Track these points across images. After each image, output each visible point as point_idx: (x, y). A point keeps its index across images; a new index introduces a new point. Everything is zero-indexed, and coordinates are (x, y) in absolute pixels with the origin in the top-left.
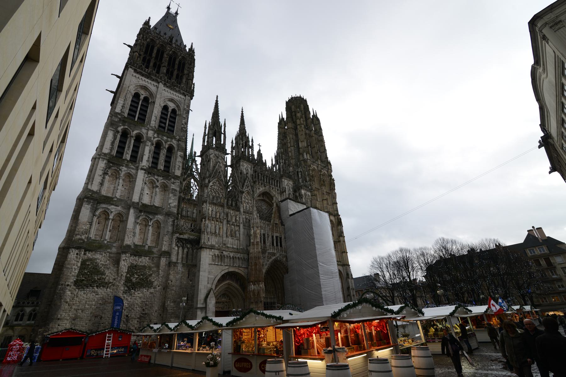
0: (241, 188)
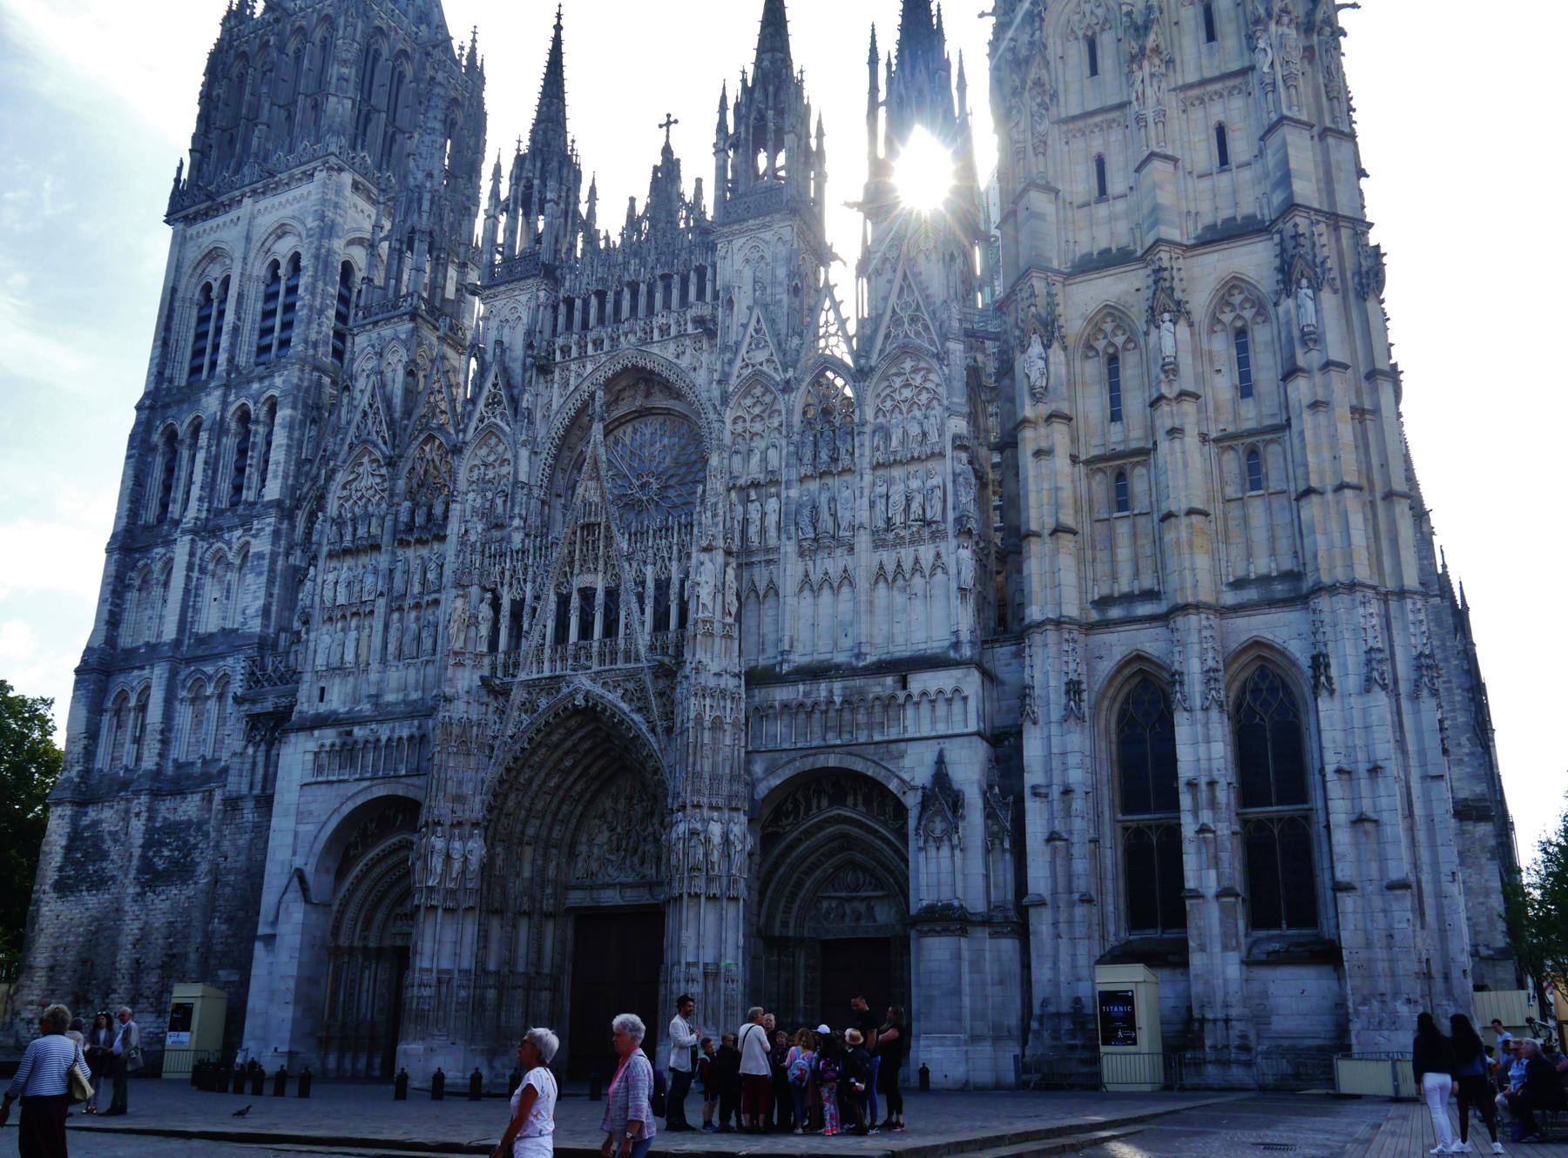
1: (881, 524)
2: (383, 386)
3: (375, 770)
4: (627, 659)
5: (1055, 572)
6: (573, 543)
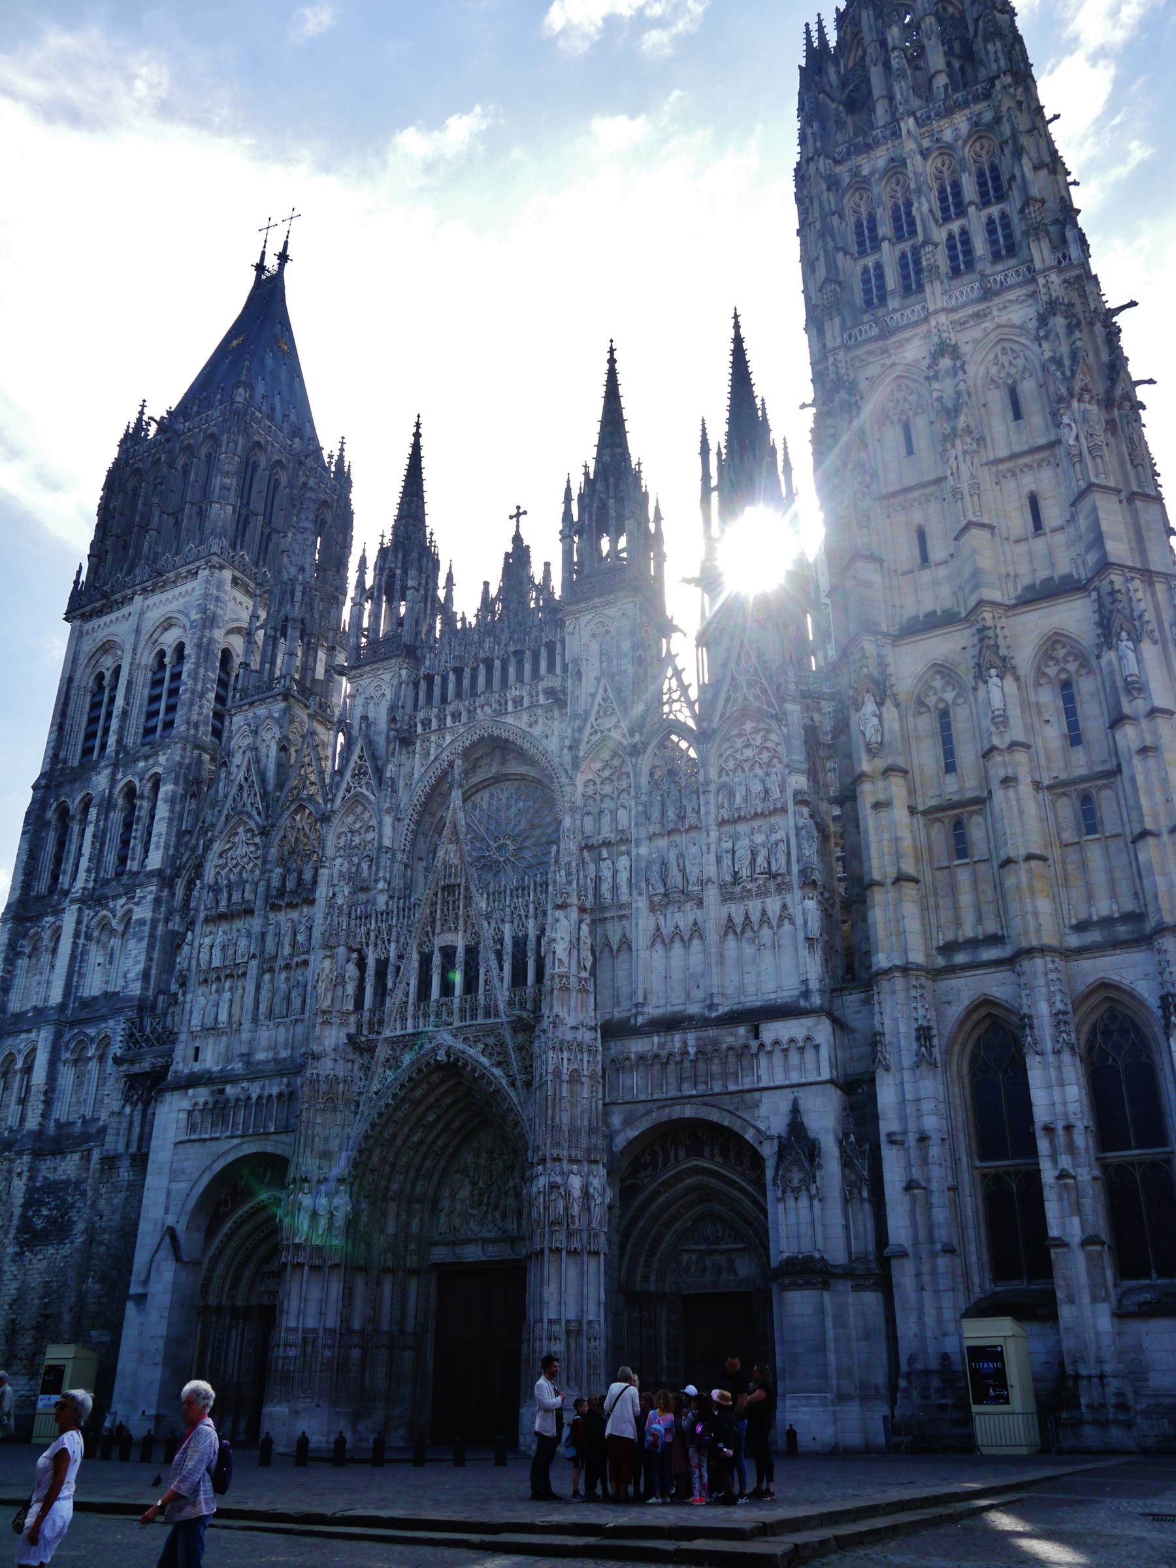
1: (728, 878)
2: (258, 761)
3: (245, 1128)
4: (487, 1015)
5: (899, 919)
6: (434, 904)
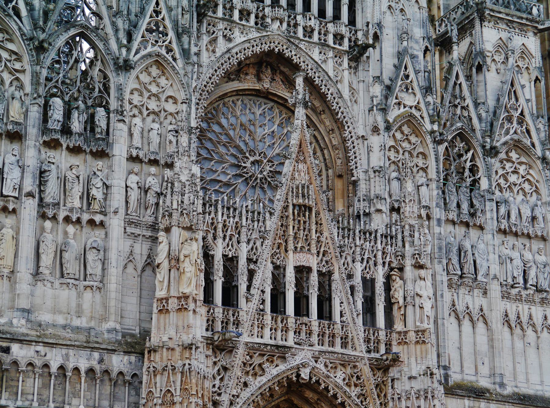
0: (120, 46)
1: (510, 280)
